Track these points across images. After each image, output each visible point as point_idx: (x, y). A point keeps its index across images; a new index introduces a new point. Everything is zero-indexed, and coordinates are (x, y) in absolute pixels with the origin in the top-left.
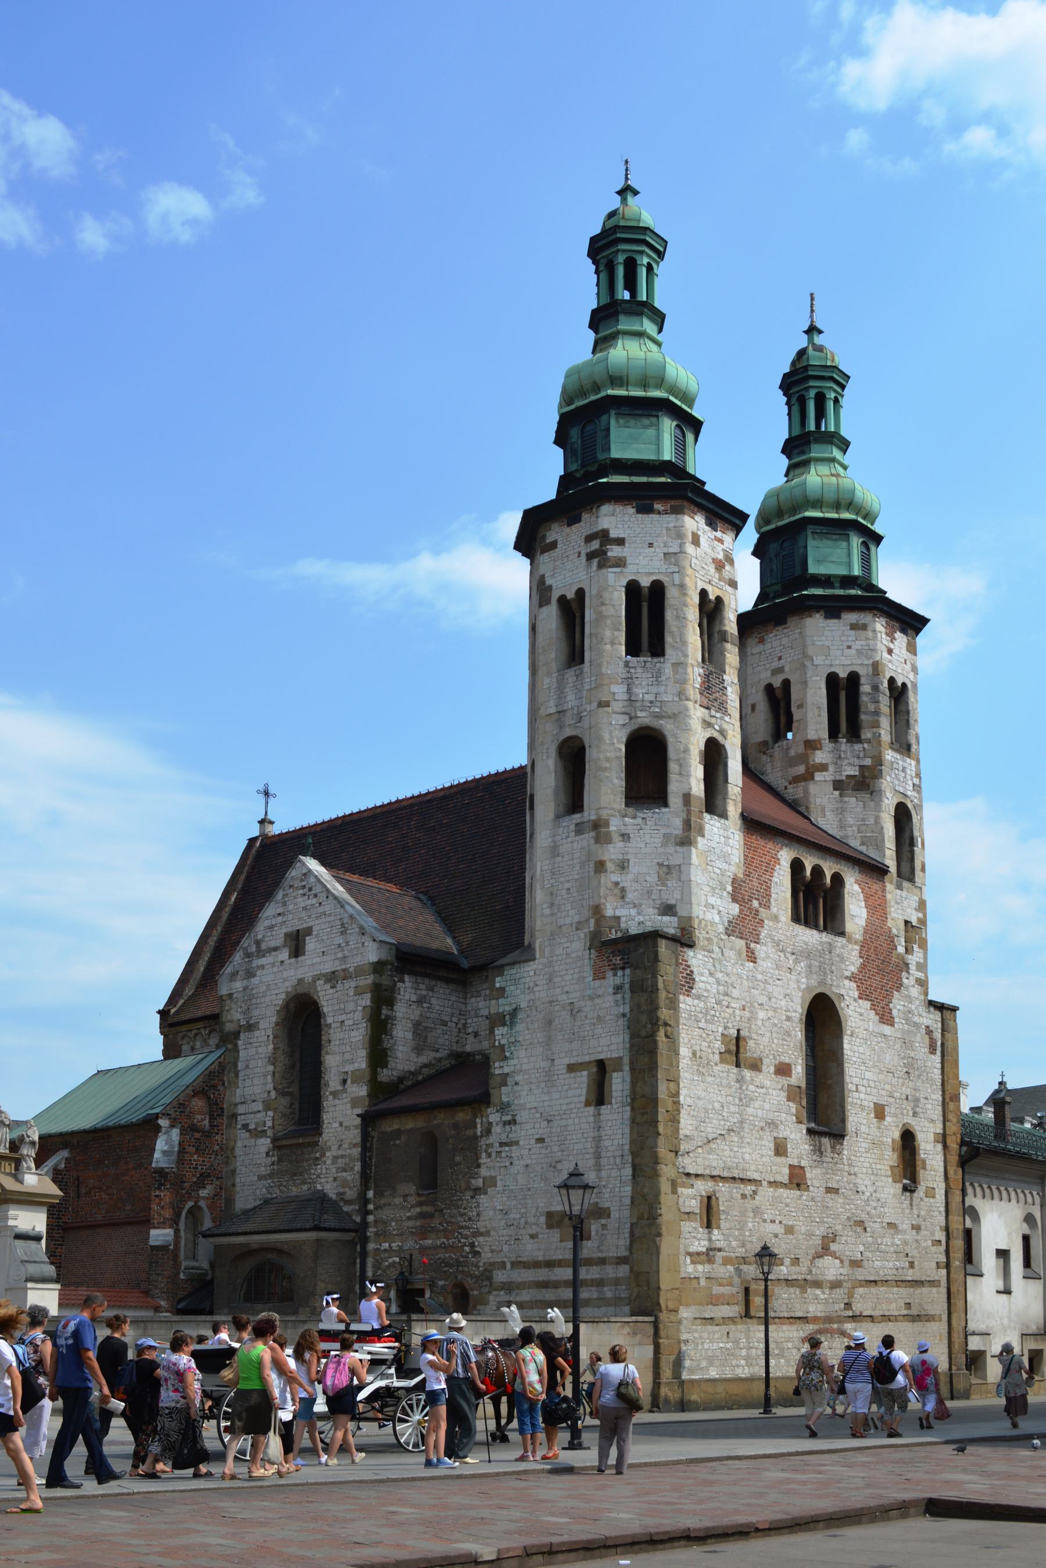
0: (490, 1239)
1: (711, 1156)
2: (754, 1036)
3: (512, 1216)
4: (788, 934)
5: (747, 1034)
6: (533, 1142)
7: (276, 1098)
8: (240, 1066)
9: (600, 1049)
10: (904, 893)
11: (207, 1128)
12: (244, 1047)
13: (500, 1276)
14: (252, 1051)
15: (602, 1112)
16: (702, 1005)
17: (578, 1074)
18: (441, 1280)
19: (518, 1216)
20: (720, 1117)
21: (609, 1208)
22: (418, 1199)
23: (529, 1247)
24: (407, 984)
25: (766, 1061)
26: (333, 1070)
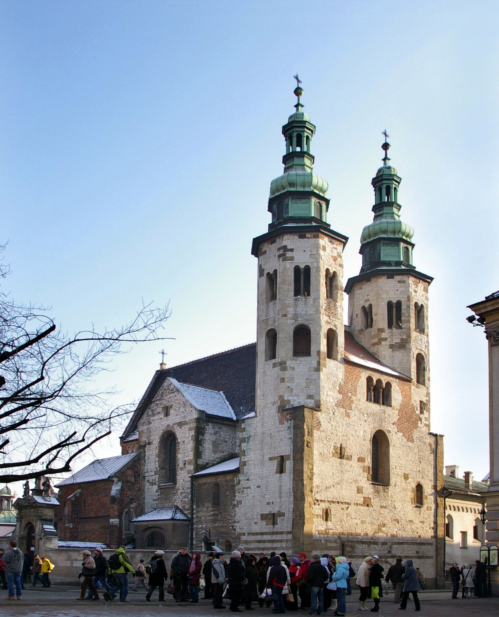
0: (239, 524)
3: (248, 515)
6: (256, 487)
8: (146, 458)
9: (282, 452)
11: (133, 481)
13: (244, 538)
14: (151, 453)
17: (273, 461)
22: (212, 509)
26: (181, 460)
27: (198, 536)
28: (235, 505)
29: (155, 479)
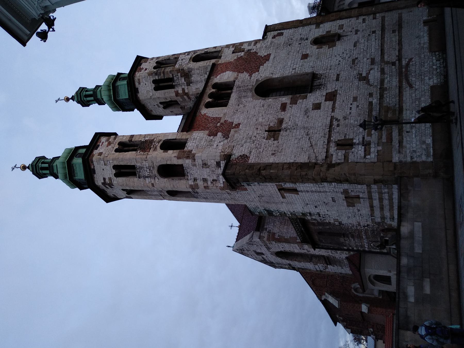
1: (318, 144)
2: (268, 123)
4: (231, 108)
5: (267, 127)
8: (303, 268)
9: (274, 190)
10: (223, 55)
13: (379, 220)
16: (253, 150)
20: (301, 139)
24: (268, 227)
25: (279, 117)
28: (339, 223)
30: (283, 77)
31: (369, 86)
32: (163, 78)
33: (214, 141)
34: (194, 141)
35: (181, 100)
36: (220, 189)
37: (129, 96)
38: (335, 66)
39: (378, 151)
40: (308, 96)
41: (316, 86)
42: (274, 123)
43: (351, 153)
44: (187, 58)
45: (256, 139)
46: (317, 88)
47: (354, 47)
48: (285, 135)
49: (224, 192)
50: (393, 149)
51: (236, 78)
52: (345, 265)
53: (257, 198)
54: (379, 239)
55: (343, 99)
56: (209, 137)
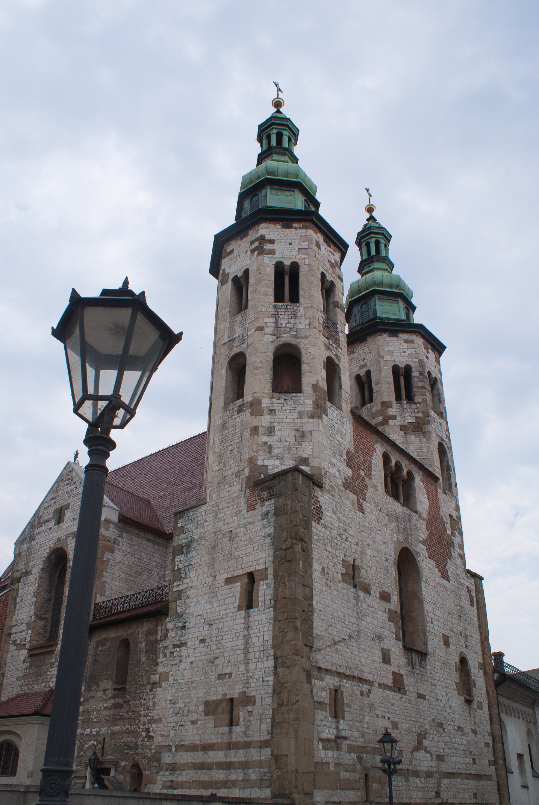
0: (162, 725)
1: (337, 656)
2: (365, 567)
3: (179, 705)
5: (360, 564)
6: (198, 641)
7: (34, 621)
8: (18, 600)
9: (250, 564)
10: (448, 497)
12: (22, 587)
13: (167, 758)
14: (26, 590)
15: (251, 614)
16: (328, 533)
17: (234, 585)
18: (123, 761)
19: (183, 705)
20: (343, 625)
21: (255, 696)
23: (190, 732)
25: (373, 588)
27: (82, 753)
29: (26, 638)
30: (422, 601)
31: (410, 750)
32: (415, 385)
33: (340, 461)
34: (339, 423)
35: (374, 410)
36: (250, 456)
37: (381, 318)
38: (435, 693)
39: (328, 763)
40: (398, 641)
41: (412, 657)
42: (365, 576)
43: (325, 714)
44: (443, 434)
45: (344, 540)
46: (409, 659)
47: (458, 727)
48: (350, 596)
49: (244, 464)
50: (331, 791)
51: (420, 516)
52: (28, 684)
53: (225, 527)
54: (109, 757)
55: (395, 705)
56: (346, 451)
